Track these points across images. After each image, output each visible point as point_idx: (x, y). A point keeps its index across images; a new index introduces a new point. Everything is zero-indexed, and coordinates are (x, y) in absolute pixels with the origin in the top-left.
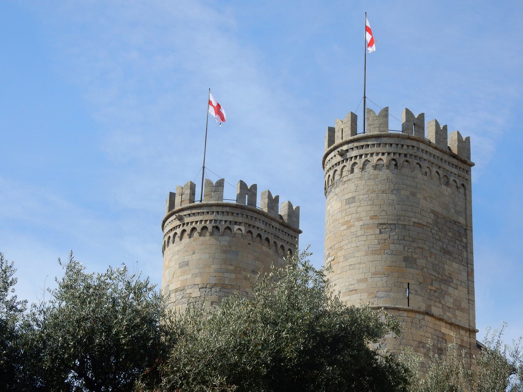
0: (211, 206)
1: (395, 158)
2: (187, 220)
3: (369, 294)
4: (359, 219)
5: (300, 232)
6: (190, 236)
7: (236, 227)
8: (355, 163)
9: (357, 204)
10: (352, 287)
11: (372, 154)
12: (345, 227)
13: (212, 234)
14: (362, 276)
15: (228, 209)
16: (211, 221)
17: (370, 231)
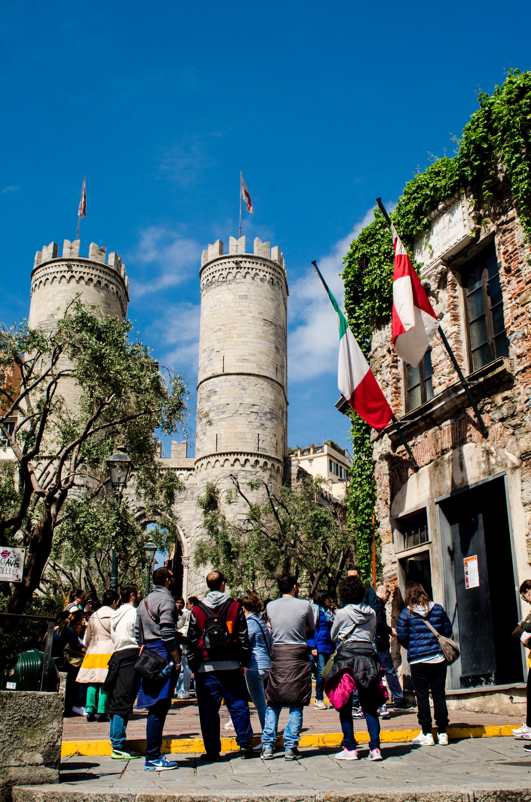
0: (95, 263)
1: (273, 277)
2: (75, 268)
3: (258, 365)
4: (250, 312)
6: (78, 282)
7: (111, 286)
8: (248, 273)
9: (249, 301)
10: (245, 357)
11: (260, 270)
12: (239, 314)
13: (95, 286)
14: (252, 352)
16: (96, 276)
17: (258, 323)
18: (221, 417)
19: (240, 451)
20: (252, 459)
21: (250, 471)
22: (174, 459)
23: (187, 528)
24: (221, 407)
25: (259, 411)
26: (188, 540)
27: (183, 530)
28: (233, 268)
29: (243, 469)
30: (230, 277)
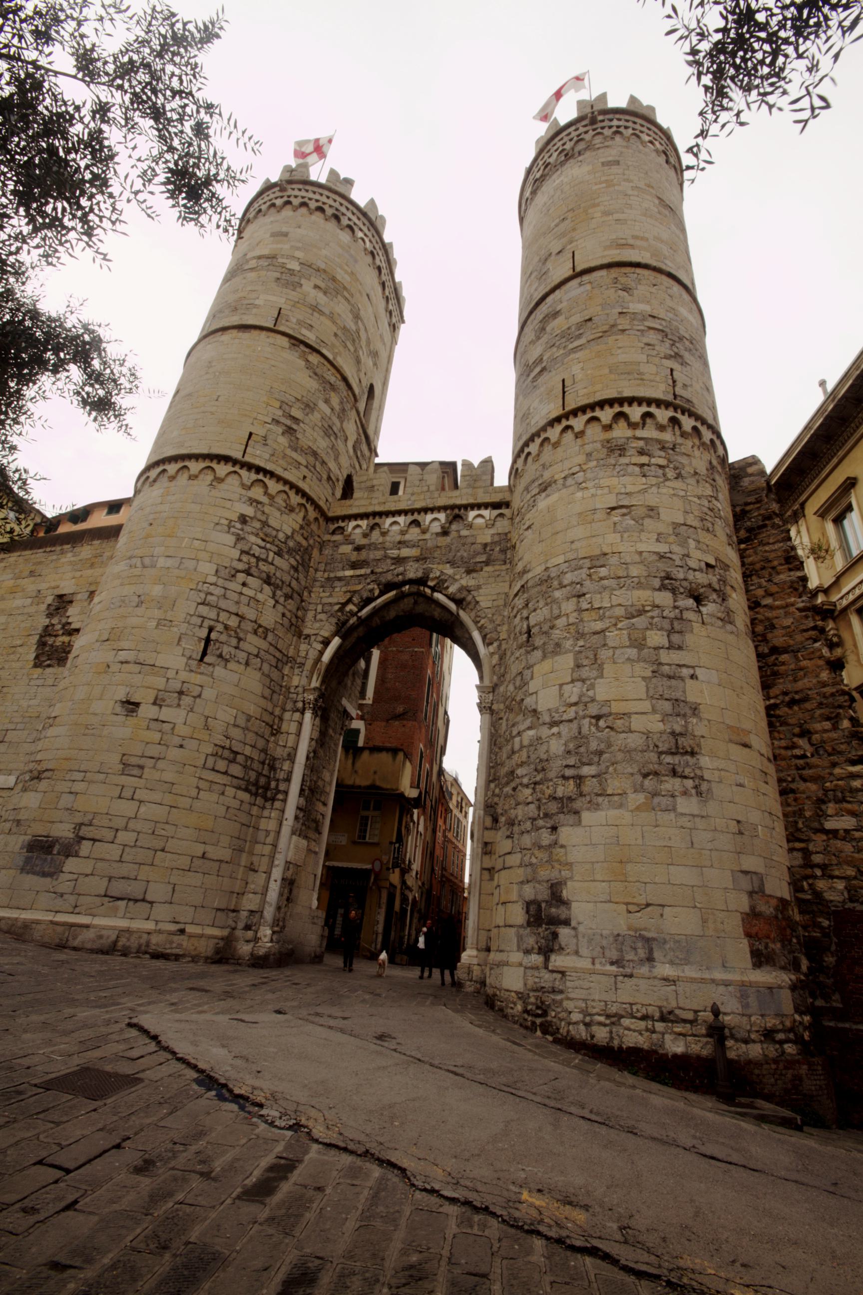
5: (403, 322)
7: (360, 234)
10: (623, 242)
11: (642, 132)
15: (355, 211)
16: (331, 206)
18: (571, 346)
19: (627, 393)
20: (663, 415)
21: (658, 441)
22: (464, 491)
23: (492, 621)
24: (573, 328)
25: (667, 330)
26: (491, 649)
27: (480, 629)
28: (586, 132)
29: (639, 433)
30: (581, 146)
